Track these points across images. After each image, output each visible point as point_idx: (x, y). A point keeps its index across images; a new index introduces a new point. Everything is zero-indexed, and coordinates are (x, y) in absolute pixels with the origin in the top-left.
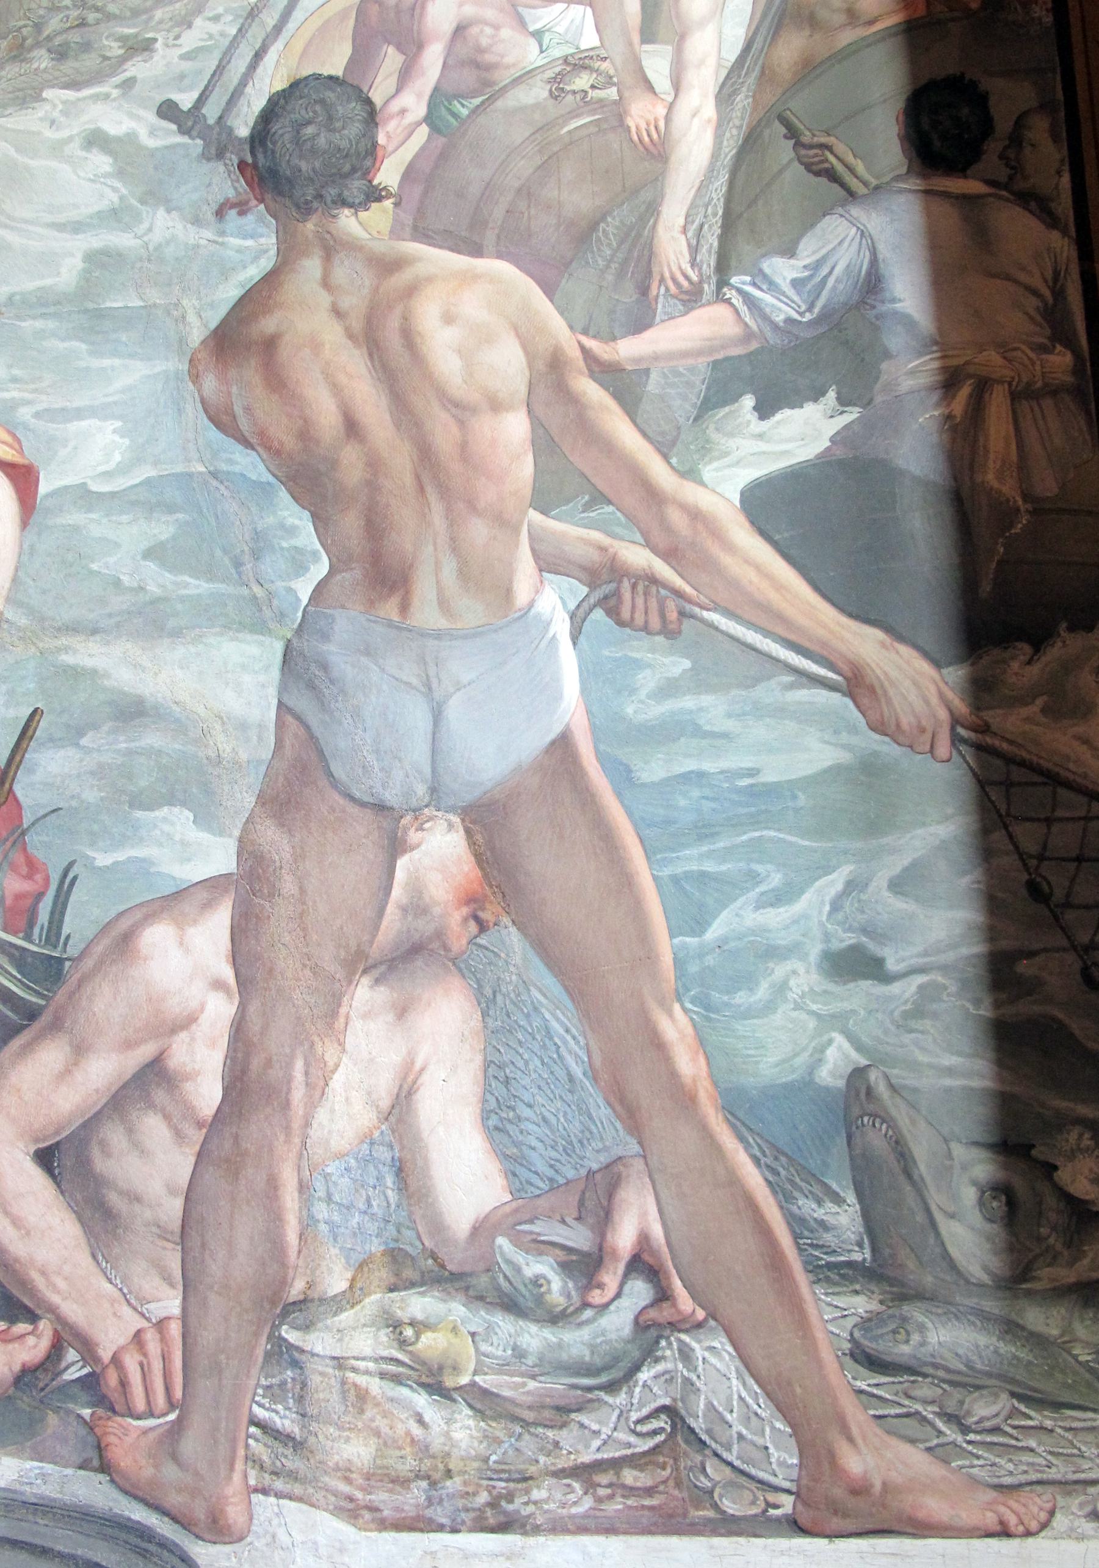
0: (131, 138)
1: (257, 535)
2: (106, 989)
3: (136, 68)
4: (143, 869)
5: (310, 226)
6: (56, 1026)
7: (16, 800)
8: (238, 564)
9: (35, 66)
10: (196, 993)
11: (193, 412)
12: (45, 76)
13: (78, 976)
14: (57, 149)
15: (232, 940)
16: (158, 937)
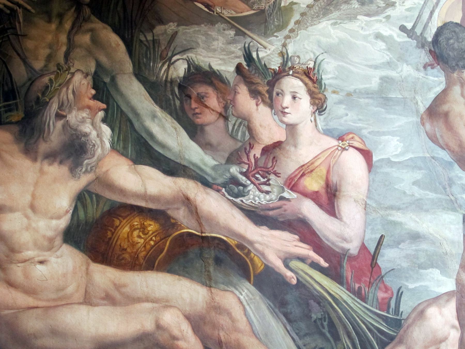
0: (391, 37)
1: (450, 179)
2: (417, 329)
3: (389, 12)
4: (426, 288)
5: (455, 75)
6: (401, 342)
7: (379, 266)
8: (445, 188)
9: (353, 6)
10: (447, 329)
11: (424, 135)
12: (357, 10)
13: (407, 325)
14: (365, 38)
15: (457, 312)
16: (432, 311)
